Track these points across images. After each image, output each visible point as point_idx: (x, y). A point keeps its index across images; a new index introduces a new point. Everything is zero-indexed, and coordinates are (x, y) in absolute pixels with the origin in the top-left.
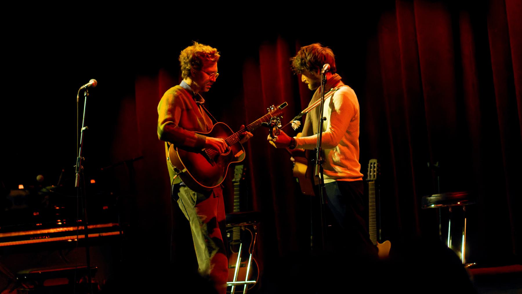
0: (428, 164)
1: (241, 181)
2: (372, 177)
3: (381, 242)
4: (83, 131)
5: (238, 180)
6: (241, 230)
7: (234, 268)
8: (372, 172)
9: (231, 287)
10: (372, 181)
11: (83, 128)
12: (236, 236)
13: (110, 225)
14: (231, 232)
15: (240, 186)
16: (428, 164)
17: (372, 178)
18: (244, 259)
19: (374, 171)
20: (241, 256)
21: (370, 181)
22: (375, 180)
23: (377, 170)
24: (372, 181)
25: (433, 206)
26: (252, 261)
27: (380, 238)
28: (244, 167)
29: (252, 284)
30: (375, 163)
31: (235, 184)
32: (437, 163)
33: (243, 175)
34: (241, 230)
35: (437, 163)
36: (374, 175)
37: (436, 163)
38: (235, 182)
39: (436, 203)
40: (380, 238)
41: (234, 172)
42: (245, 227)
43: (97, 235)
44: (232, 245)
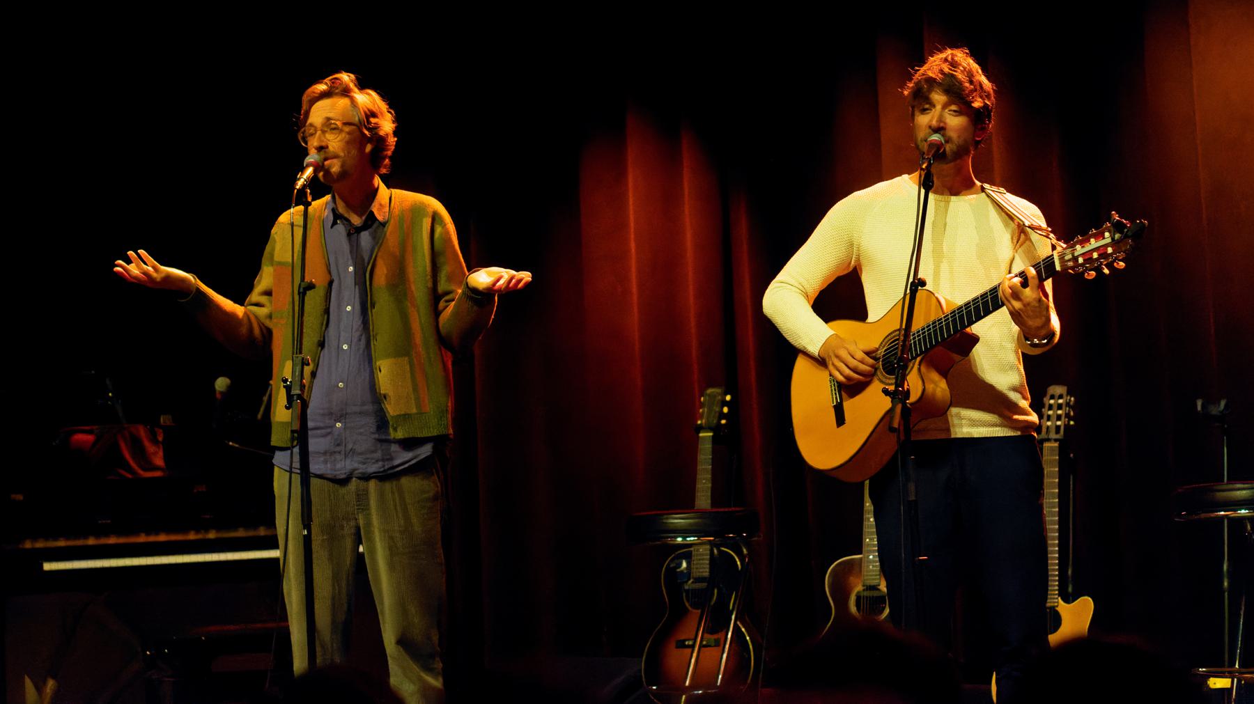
0: (1199, 403)
2: (1053, 430)
3: (1068, 599)
6: (712, 551)
10: (1056, 440)
12: (703, 568)
14: (688, 556)
16: (1199, 403)
21: (1048, 440)
23: (1067, 415)
24: (1056, 440)
27: (1070, 589)
30: (1061, 397)
32: (1223, 403)
35: (1223, 403)
40: (1070, 589)
44: (687, 591)
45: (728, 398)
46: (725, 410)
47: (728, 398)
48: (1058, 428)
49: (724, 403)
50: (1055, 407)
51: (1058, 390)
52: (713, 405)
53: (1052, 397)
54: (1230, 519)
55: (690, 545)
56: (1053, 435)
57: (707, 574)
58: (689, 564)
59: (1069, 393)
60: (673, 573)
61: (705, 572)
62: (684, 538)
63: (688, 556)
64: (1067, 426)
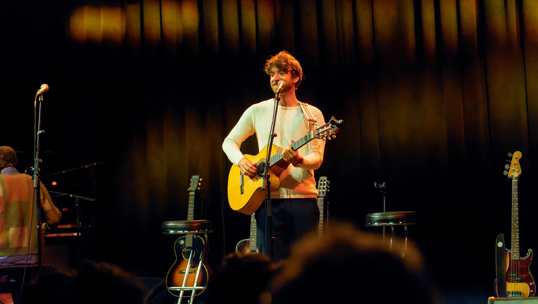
0: (375, 184)
1: (196, 191)
2: (322, 193)
4: (40, 134)
5: (194, 189)
6: (193, 237)
7: (184, 273)
8: (322, 189)
9: (180, 292)
11: (40, 132)
12: (189, 242)
13: (69, 226)
15: (196, 195)
16: (375, 184)
17: (321, 195)
18: (194, 265)
19: (324, 189)
20: (191, 263)
22: (324, 197)
23: (327, 188)
25: (376, 224)
26: (202, 268)
28: (200, 178)
29: (200, 290)
30: (325, 181)
31: (190, 193)
32: (384, 184)
33: (198, 186)
34: (193, 237)
35: (384, 184)
36: (323, 192)
37: (382, 184)
38: (190, 191)
39: (380, 221)
41: (190, 182)
42: (197, 234)
43: (55, 235)
44: (184, 252)
45: (201, 180)
46: (200, 184)
47: (201, 180)
48: (323, 192)
49: (199, 182)
50: (322, 185)
51: (324, 178)
52: (195, 181)
53: (321, 181)
54: (386, 226)
55: (185, 234)
56: (321, 195)
57: (191, 246)
58: (185, 242)
59: (328, 179)
60: (178, 245)
61: (191, 245)
62: (183, 231)
63: (184, 239)
64: (327, 192)
